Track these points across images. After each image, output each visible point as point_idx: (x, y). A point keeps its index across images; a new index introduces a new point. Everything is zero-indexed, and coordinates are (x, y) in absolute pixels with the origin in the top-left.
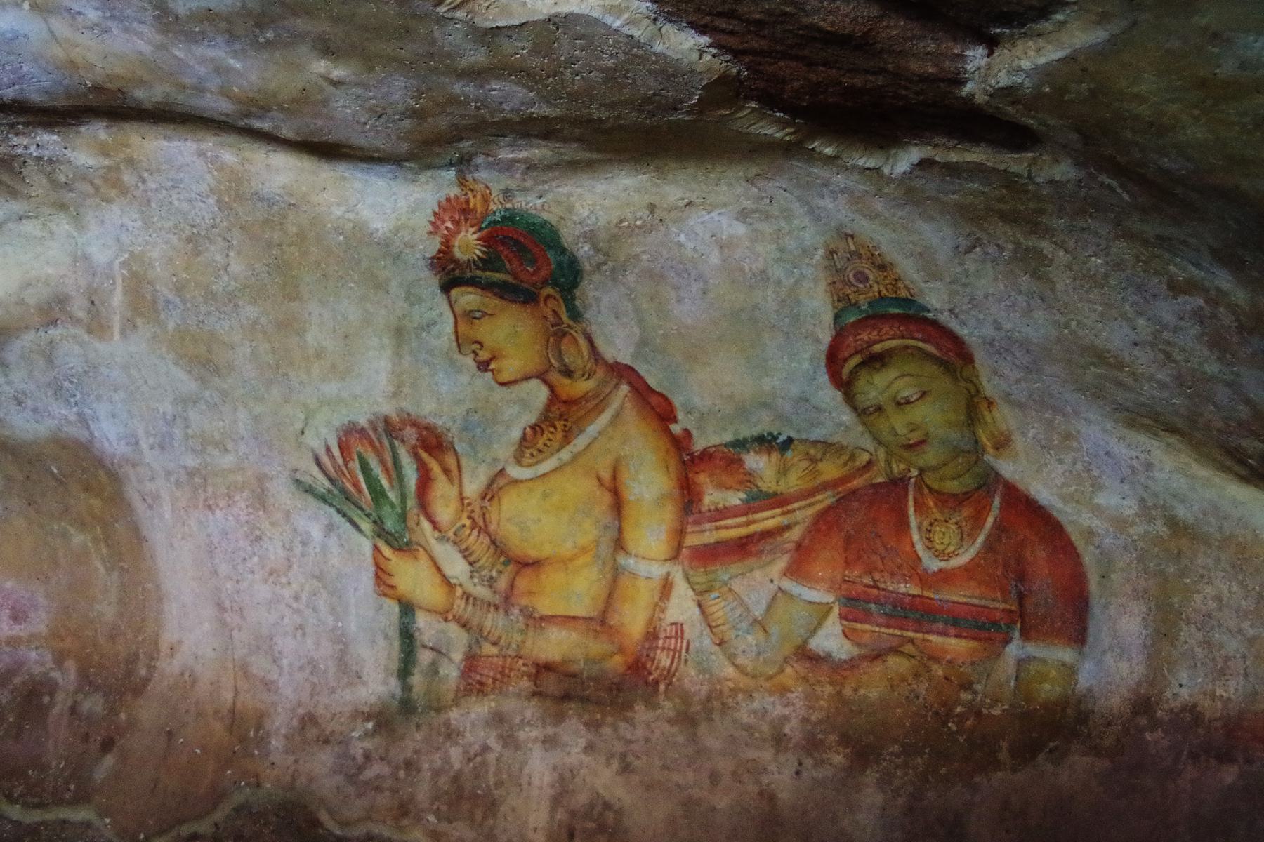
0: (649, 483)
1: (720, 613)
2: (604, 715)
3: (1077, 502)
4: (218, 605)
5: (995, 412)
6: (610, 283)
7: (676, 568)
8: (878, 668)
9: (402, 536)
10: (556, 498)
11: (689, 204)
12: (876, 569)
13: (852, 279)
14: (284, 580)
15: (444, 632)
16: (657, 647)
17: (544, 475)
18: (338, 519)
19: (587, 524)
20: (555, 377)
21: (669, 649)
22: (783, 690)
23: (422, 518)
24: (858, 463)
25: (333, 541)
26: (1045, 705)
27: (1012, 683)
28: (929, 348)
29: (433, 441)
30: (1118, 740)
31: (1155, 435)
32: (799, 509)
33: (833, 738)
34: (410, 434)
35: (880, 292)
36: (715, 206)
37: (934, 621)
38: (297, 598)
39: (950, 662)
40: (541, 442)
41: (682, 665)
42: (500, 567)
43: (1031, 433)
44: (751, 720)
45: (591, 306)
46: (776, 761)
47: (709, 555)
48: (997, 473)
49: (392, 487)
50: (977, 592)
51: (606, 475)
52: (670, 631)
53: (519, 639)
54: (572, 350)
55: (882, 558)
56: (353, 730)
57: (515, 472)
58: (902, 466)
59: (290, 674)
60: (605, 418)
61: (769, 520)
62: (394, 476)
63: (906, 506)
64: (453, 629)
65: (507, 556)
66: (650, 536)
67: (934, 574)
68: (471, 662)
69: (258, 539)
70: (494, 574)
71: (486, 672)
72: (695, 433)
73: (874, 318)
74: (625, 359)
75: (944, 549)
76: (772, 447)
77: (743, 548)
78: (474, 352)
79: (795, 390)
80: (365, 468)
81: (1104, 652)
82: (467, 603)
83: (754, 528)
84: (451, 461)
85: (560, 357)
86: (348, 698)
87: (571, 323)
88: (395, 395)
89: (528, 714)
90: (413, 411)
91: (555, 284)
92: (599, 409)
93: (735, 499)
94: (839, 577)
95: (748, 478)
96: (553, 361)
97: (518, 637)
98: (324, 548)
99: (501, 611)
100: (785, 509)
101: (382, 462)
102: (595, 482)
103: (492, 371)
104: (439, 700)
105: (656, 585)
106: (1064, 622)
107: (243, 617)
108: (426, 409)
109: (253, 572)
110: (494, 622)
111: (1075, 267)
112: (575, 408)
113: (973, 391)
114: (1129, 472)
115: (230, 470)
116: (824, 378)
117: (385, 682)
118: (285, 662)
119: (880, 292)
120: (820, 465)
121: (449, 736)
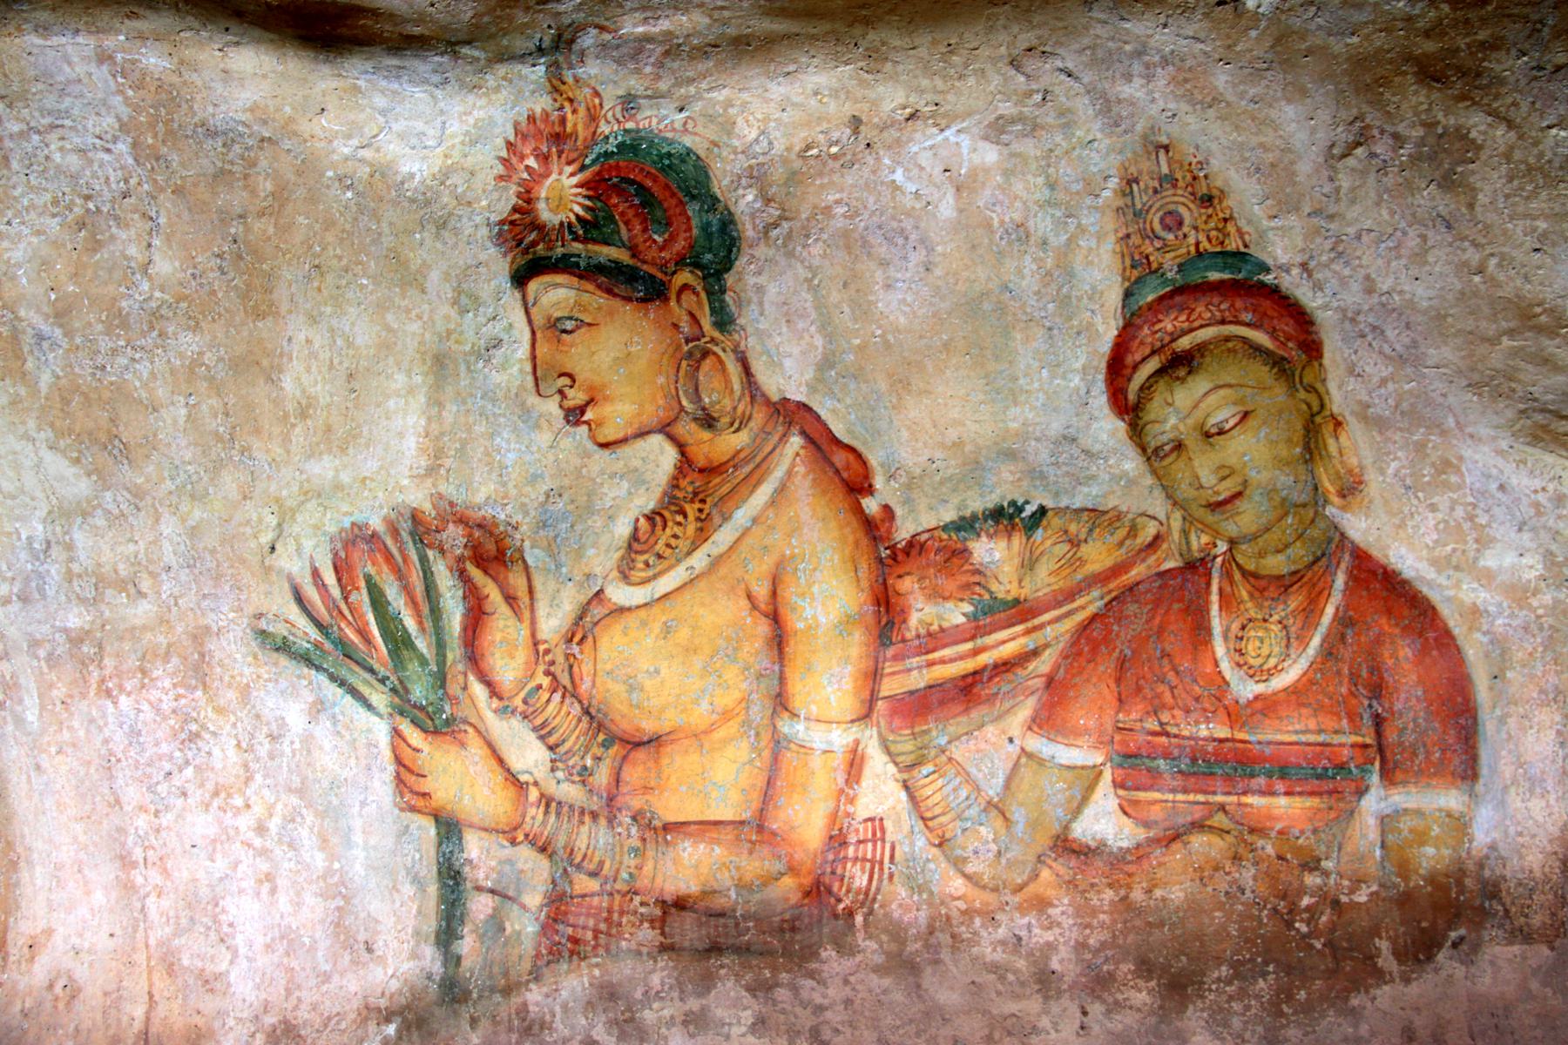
0: (828, 598)
1: (937, 798)
3: (1457, 568)
4: (122, 858)
5: (1343, 439)
6: (783, 261)
7: (868, 732)
8: (1177, 854)
10: (684, 634)
13: (1157, 226)
14: (238, 801)
15: (509, 861)
16: (845, 858)
17: (665, 596)
18: (332, 691)
19: (731, 673)
20: (687, 429)
21: (864, 860)
23: (471, 678)
24: (1139, 541)
26: (1431, 879)
27: (1378, 853)
28: (1261, 338)
29: (490, 547)
30: (1553, 914)
32: (1049, 623)
33: (1126, 967)
34: (455, 536)
35: (1197, 244)
37: (1252, 776)
38: (261, 829)
39: (1280, 832)
40: (664, 537)
41: (886, 882)
42: (598, 751)
43: (1394, 465)
44: (999, 956)
45: (749, 302)
46: (1046, 1012)
47: (920, 706)
48: (1342, 534)
49: (423, 630)
50: (1312, 724)
51: (762, 591)
52: (865, 831)
53: (633, 863)
54: (717, 383)
55: (1172, 688)
57: (620, 594)
58: (1205, 539)
59: (249, 959)
61: (1006, 643)
62: (426, 610)
63: (1208, 602)
64: (526, 857)
66: (828, 684)
67: (1250, 703)
68: (558, 905)
69: (194, 737)
70: (589, 762)
71: (582, 921)
72: (899, 511)
73: (1184, 293)
74: (797, 394)
75: (1264, 662)
76: (1013, 527)
77: (968, 691)
78: (560, 392)
79: (1056, 427)
81: (1506, 789)
82: (546, 812)
83: (985, 659)
84: (517, 581)
87: (716, 334)
88: (431, 471)
89: (656, 980)
90: (459, 497)
91: (697, 265)
92: (753, 480)
94: (1109, 727)
95: (977, 578)
96: (685, 403)
98: (308, 739)
99: (603, 821)
100: (1029, 624)
101: (407, 589)
102: (744, 603)
103: (587, 423)
104: (506, 974)
105: (839, 760)
106: (1444, 751)
107: (165, 872)
108: (481, 493)
109: (184, 794)
110: (593, 839)
111: (1517, 155)
112: (717, 480)
114: (1532, 512)
115: (145, 628)
117: (414, 956)
118: (239, 940)
119: (1197, 244)
120: (1084, 549)
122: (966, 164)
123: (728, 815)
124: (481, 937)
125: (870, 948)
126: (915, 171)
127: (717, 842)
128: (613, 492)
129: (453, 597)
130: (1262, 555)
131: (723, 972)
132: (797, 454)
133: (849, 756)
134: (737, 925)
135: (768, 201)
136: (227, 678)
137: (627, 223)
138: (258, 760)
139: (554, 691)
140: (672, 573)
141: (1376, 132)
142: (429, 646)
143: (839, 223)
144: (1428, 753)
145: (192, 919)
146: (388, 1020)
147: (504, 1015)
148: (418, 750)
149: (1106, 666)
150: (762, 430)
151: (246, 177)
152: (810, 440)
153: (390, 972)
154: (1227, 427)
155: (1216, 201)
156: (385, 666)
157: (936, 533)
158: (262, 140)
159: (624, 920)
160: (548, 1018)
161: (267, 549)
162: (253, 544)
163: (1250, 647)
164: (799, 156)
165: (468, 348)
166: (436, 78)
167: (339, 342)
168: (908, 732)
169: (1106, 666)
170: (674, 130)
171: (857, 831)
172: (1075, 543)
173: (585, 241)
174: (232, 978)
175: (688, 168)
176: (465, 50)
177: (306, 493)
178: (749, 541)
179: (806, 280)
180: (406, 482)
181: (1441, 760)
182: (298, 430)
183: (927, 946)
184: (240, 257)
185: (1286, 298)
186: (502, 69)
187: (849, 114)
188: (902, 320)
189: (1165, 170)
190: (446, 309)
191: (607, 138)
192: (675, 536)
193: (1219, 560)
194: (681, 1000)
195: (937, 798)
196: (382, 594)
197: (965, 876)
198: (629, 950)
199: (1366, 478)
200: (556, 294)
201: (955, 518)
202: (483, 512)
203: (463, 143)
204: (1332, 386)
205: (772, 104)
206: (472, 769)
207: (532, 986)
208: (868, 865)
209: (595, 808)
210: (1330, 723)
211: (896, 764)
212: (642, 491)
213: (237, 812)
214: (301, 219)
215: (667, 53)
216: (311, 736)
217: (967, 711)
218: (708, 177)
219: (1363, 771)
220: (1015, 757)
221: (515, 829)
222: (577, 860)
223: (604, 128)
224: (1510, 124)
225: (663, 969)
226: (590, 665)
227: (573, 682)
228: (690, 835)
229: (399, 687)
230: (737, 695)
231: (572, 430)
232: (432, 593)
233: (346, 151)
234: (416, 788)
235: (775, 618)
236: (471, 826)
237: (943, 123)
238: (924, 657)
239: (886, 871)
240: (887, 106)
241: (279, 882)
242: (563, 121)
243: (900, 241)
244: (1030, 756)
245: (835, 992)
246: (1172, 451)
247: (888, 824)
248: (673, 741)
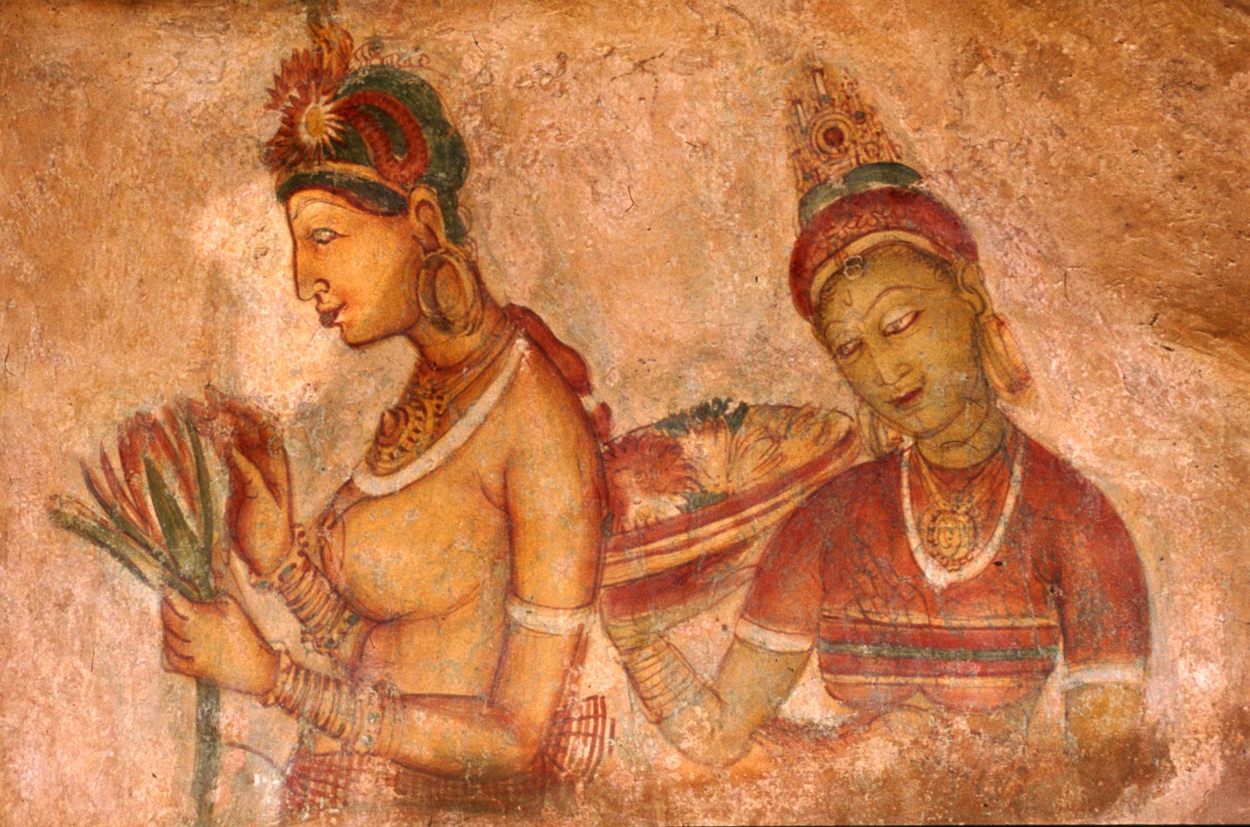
0: (554, 492)
1: (657, 679)
3: (1119, 457)
5: (1007, 338)
7: (592, 618)
12: (865, 594)
13: (821, 141)
16: (570, 733)
18: (113, 564)
20: (426, 331)
21: (587, 735)
22: (751, 777)
23: (233, 554)
24: (833, 436)
29: (255, 436)
31: (1205, 345)
32: (757, 515)
34: (223, 426)
35: (857, 157)
42: (344, 627)
43: (1055, 364)
47: (640, 595)
48: (1015, 427)
51: (493, 480)
53: (372, 728)
54: (452, 290)
55: (872, 578)
58: (892, 434)
60: (492, 394)
61: (718, 534)
62: (197, 493)
63: (899, 497)
67: (943, 591)
70: (335, 636)
72: (615, 410)
77: (683, 582)
78: (317, 296)
80: (156, 486)
81: (1175, 660)
82: (295, 679)
83: (697, 550)
84: (279, 471)
85: (435, 304)
91: (431, 182)
92: (483, 381)
93: (671, 507)
94: (814, 616)
95: (689, 473)
96: (424, 308)
98: (91, 609)
99: (345, 689)
100: (738, 517)
101: (181, 473)
102: (479, 495)
103: (339, 325)
105: (565, 641)
106: (1119, 629)
112: (452, 379)
113: (979, 308)
116: (788, 303)
119: (857, 157)
120: (785, 446)
129: (220, 481)
130: (945, 447)
134: (465, 786)
137: (372, 144)
140: (414, 465)
141: (989, 52)
142: (198, 527)
143: (552, 144)
144: (1105, 630)
148: (183, 618)
149: (810, 558)
150: (492, 334)
152: (534, 343)
154: (902, 326)
155: (869, 117)
156: (158, 541)
163: (942, 538)
168: (629, 618)
169: (810, 558)
170: (411, 65)
171: (581, 708)
172: (776, 439)
173: (336, 160)
178: (482, 437)
180: (184, 376)
181: (1117, 638)
185: (939, 205)
189: (822, 91)
191: (356, 73)
192: (417, 431)
193: (906, 454)
195: (657, 679)
196: (160, 478)
197: (683, 753)
199: (1033, 374)
200: (314, 207)
201: (666, 416)
203: (239, 78)
204: (990, 286)
208: (590, 739)
210: (1017, 608)
211: (617, 647)
217: (682, 600)
218: (439, 104)
219: (1049, 651)
220: (729, 644)
221: (268, 692)
223: (354, 65)
224: (1090, 39)
228: (424, 706)
234: (179, 650)
236: (227, 688)
238: (643, 548)
242: (321, 58)
243: (605, 160)
244: (742, 641)
246: (855, 348)
247: (608, 702)
248: (411, 622)
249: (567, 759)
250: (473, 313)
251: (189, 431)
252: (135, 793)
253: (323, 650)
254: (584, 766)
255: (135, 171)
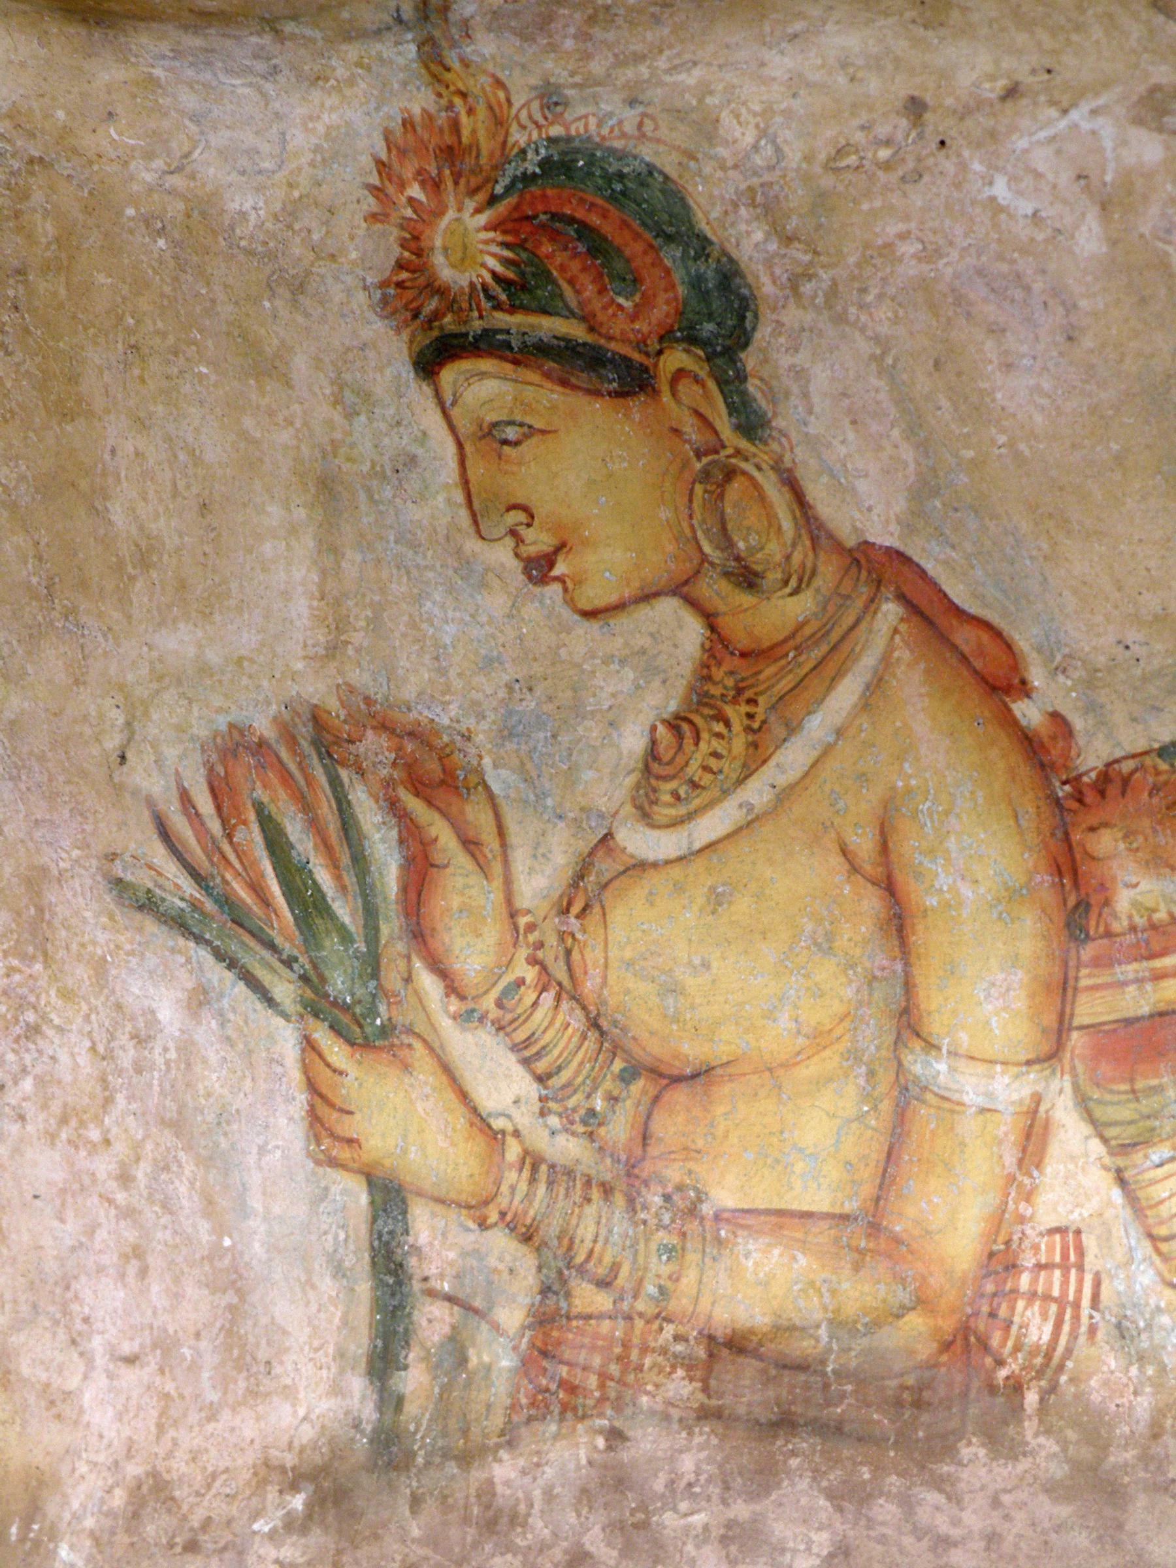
0: (975, 859)
2: (879, 1469)
7: (1055, 1084)
9: (373, 1012)
10: (743, 905)
11: (1012, 93)
14: (94, 1134)
15: (477, 1254)
16: (1015, 1291)
17: (710, 846)
18: (217, 974)
21: (1047, 1298)
23: (418, 964)
25: (206, 1032)
29: (432, 767)
36: (1079, 94)
38: (125, 1178)
41: (1082, 1339)
45: (787, 394)
49: (343, 889)
51: (864, 844)
53: (665, 1270)
54: (753, 518)
56: (256, 1515)
57: (638, 841)
60: (846, 694)
62: (345, 859)
64: (500, 1243)
65: (628, 1055)
69: (33, 1031)
72: (1078, 723)
74: (884, 535)
78: (513, 533)
82: (533, 1180)
84: (478, 816)
85: (725, 540)
86: (249, 1432)
87: (744, 444)
88: (333, 650)
89: (687, 1464)
91: (692, 340)
96: (707, 549)
97: (660, 1267)
98: (187, 1048)
99: (619, 1200)
101: (314, 824)
102: (836, 860)
103: (560, 579)
104: (465, 1432)
105: (1007, 1127)
109: (22, 1118)
110: (599, 1228)
112: (770, 671)
117: (336, 1390)
118: (97, 1343)
121: (490, 1526)
122: (1111, 166)
123: (820, 1200)
124: (435, 1369)
125: (1045, 1452)
126: (1028, 182)
127: (804, 1245)
128: (612, 685)
129: (383, 840)
131: (794, 1462)
132: (896, 631)
133: (1024, 1122)
134: (826, 1386)
135: (789, 240)
136: (74, 947)
137: (571, 282)
138: (120, 1072)
139: (544, 989)
140: (717, 812)
142: (353, 915)
143: (911, 269)
145: (35, 1306)
146: (294, 1487)
147: (460, 1495)
150: (836, 592)
151: (17, 215)
153: (301, 1412)
157: (1148, 761)
158: (31, 161)
159: (648, 1362)
160: (522, 1508)
161: (114, 758)
162: (95, 751)
164: (826, 167)
165: (366, 468)
166: (261, 66)
167: (182, 456)
168: (1125, 1087)
170: (624, 135)
171: (1036, 1248)
173: (512, 309)
174: (87, 1398)
175: (654, 194)
176: (289, 27)
177: (160, 679)
178: (832, 766)
179: (873, 357)
180: (299, 666)
182: (139, 585)
183: (1145, 1458)
184: (27, 331)
186: (352, 51)
187: (903, 94)
188: (1038, 419)
190: (324, 411)
191: (523, 152)
192: (715, 755)
194: (724, 1502)
198: (652, 1412)
200: (484, 387)
202: (413, 715)
203: (312, 164)
205: (775, 87)
206: (420, 1106)
207: (503, 1454)
208: (1054, 1308)
209: (608, 1177)
211: (1105, 1141)
212: (656, 683)
213: (93, 1148)
214: (101, 278)
215: (592, 20)
216: (193, 1043)
221: (486, 1203)
222: (579, 1259)
225: (701, 1448)
226: (599, 954)
227: (572, 976)
229: (312, 974)
230: (838, 1008)
231: (537, 590)
232: (353, 833)
233: (149, 177)
234: (339, 1131)
235: (889, 887)
236: (420, 1194)
237: (1065, 101)
238: (1145, 964)
239: (1085, 1320)
240: (965, 79)
241: (151, 1260)
242: (455, 126)
243: (1018, 294)
245: (973, 1519)
247: (1090, 1242)
248: (732, 1077)
249: (1010, 1344)
250: (797, 558)
251: (321, 759)
252: (278, 1370)
253: (581, 1129)
254: (1039, 1361)
255: (160, 325)
